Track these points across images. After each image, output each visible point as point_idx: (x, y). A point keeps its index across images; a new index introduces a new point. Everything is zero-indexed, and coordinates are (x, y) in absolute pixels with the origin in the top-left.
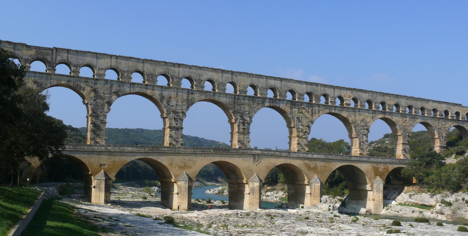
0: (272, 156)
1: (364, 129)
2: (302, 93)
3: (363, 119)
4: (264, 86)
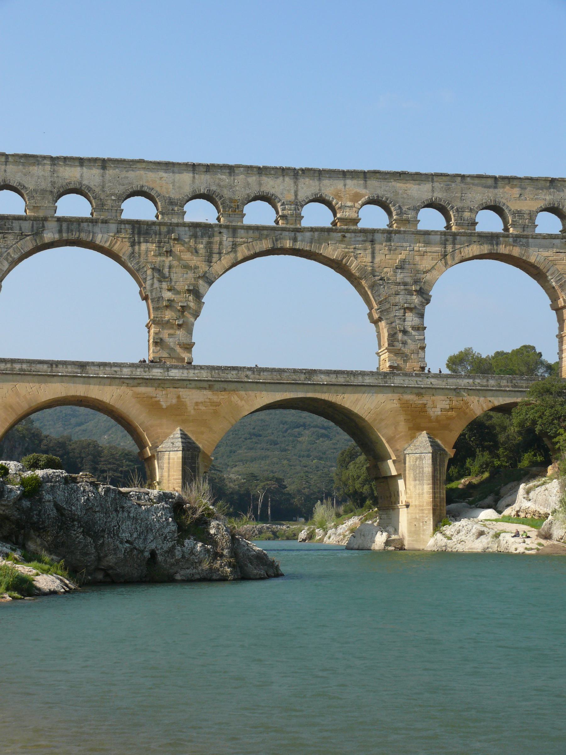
0: (22, 374)
1: (410, 293)
2: (174, 195)
3: (403, 261)
4: (45, 185)
